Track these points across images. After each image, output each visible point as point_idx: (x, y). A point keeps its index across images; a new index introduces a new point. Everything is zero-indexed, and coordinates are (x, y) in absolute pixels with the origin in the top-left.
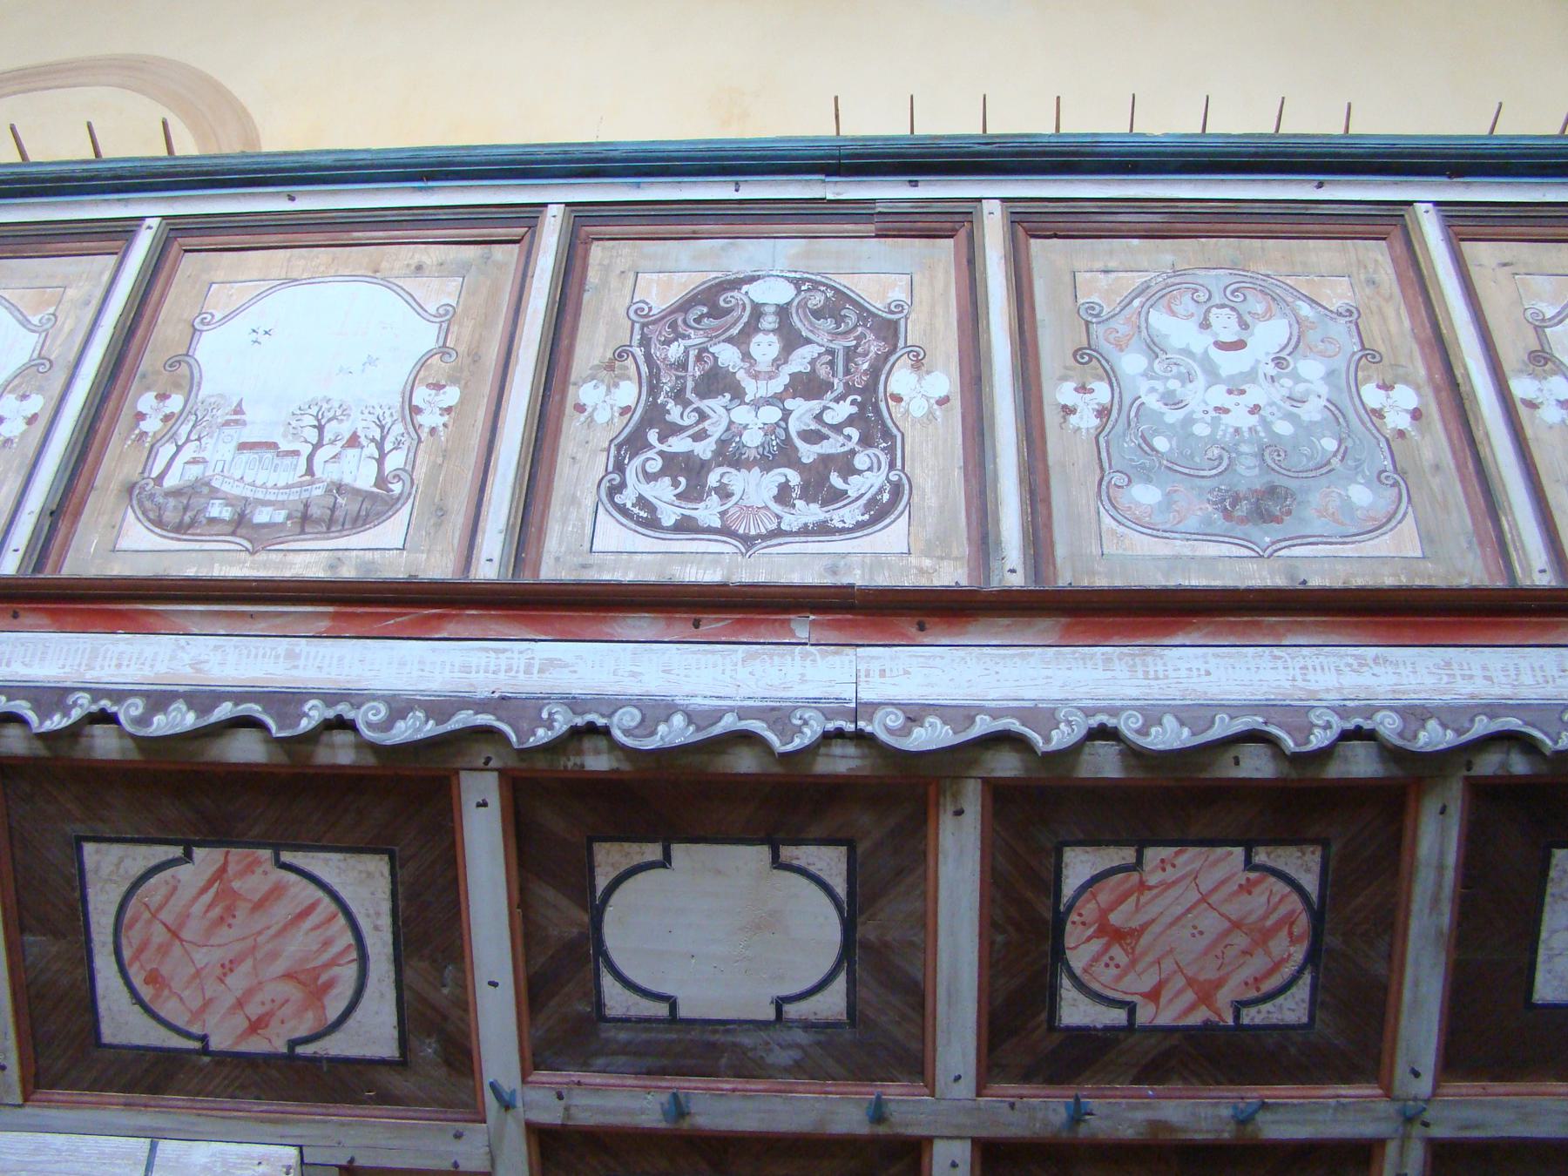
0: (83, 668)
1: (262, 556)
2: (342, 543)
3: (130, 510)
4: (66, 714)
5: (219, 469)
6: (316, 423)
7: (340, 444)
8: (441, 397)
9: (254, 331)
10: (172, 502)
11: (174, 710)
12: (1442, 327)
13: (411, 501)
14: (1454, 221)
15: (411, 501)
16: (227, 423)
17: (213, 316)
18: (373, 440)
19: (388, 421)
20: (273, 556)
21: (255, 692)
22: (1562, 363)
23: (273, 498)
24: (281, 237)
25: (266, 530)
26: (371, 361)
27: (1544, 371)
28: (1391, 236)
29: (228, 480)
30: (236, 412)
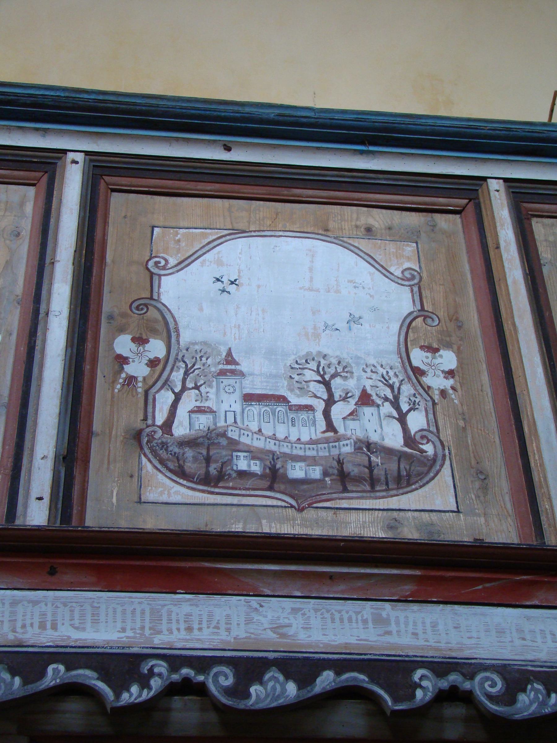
0: (147, 632)
1: (310, 514)
2: (393, 502)
3: (144, 460)
4: (145, 684)
5: (231, 420)
6: (319, 378)
7: (353, 401)
8: (438, 361)
9: (218, 280)
10: (189, 453)
11: (270, 680)
13: (447, 462)
15: (447, 462)
16: (222, 373)
17: (166, 261)
18: (386, 399)
19: (394, 380)
20: (323, 514)
21: (363, 660)
23: (301, 453)
24: (217, 186)
25: (305, 487)
26: (354, 320)
29: (246, 433)
30: (228, 363)
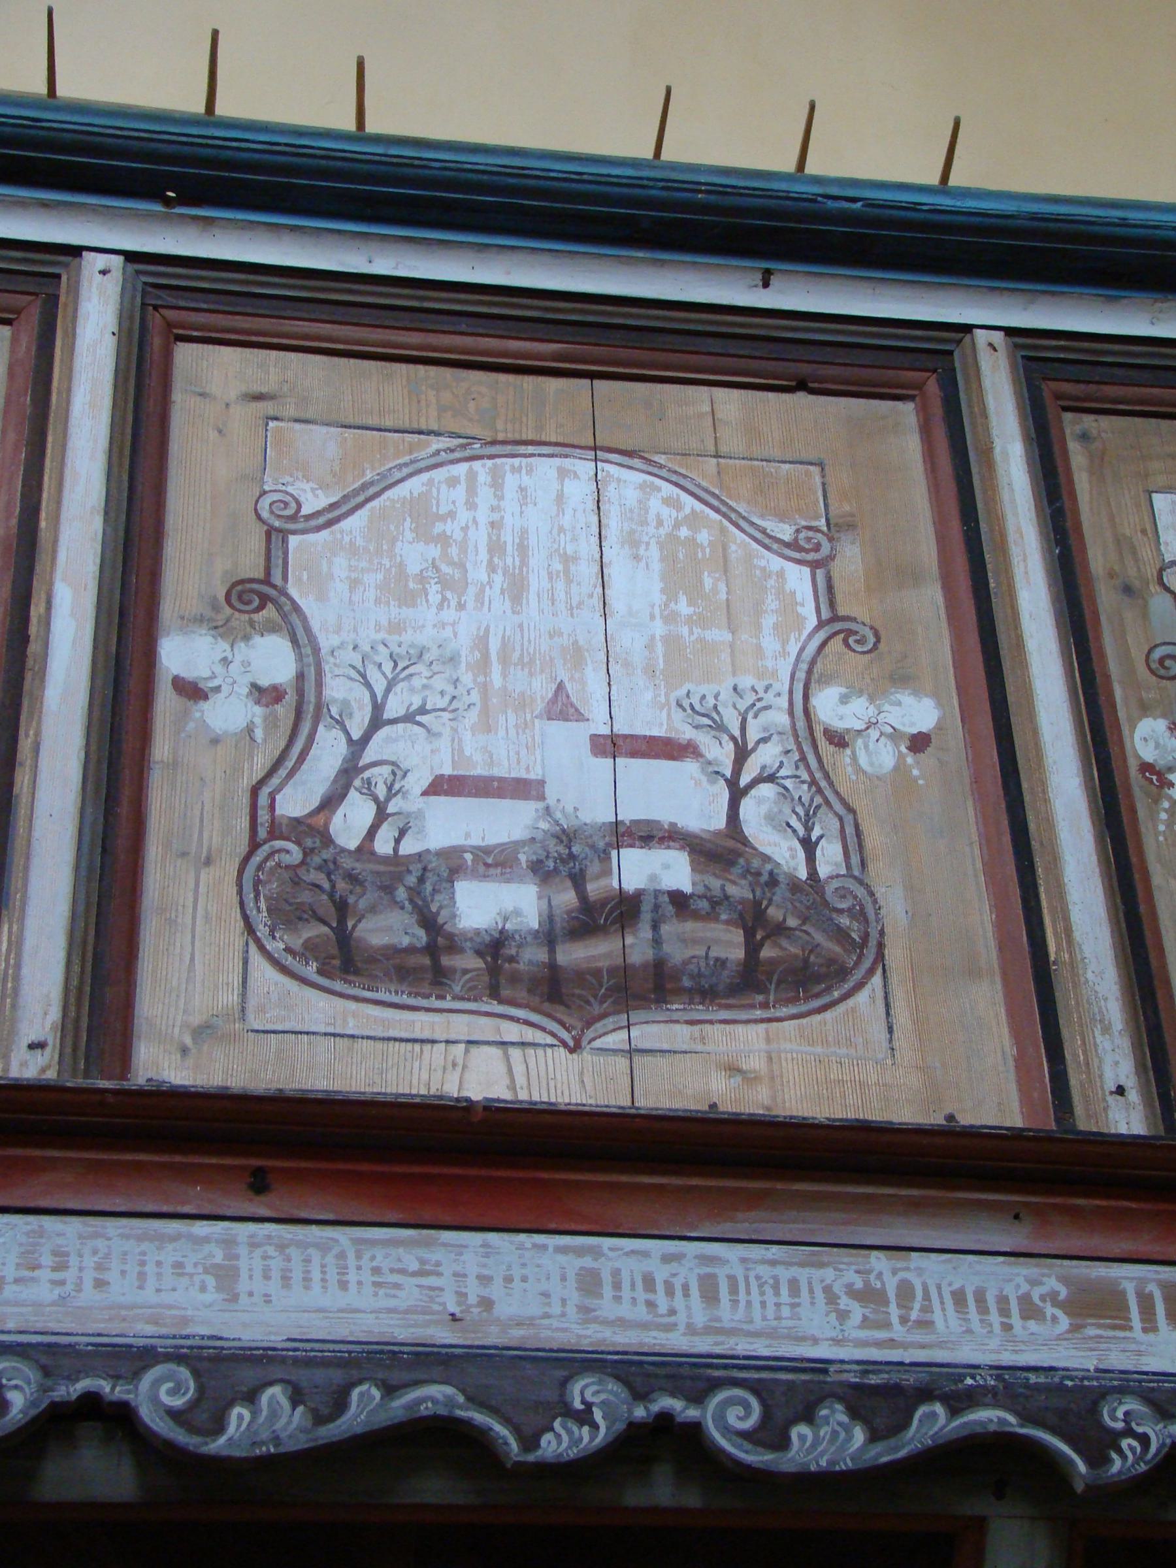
12: (43, 515)
14: (168, 298)
22: (296, 608)
27: (252, 623)
28: (23, 316)
